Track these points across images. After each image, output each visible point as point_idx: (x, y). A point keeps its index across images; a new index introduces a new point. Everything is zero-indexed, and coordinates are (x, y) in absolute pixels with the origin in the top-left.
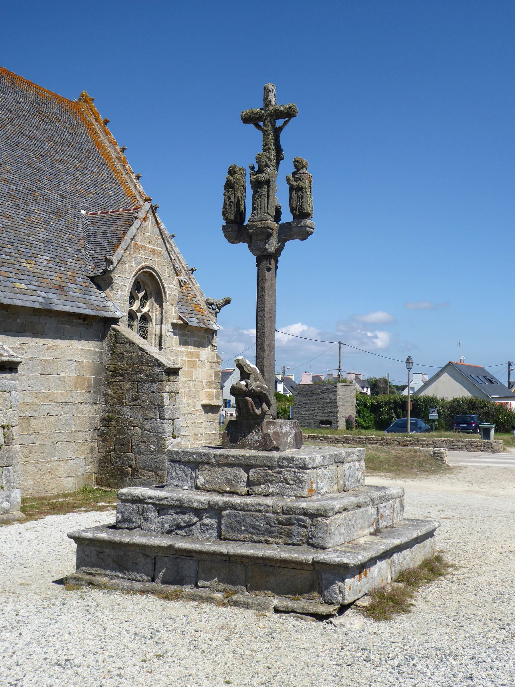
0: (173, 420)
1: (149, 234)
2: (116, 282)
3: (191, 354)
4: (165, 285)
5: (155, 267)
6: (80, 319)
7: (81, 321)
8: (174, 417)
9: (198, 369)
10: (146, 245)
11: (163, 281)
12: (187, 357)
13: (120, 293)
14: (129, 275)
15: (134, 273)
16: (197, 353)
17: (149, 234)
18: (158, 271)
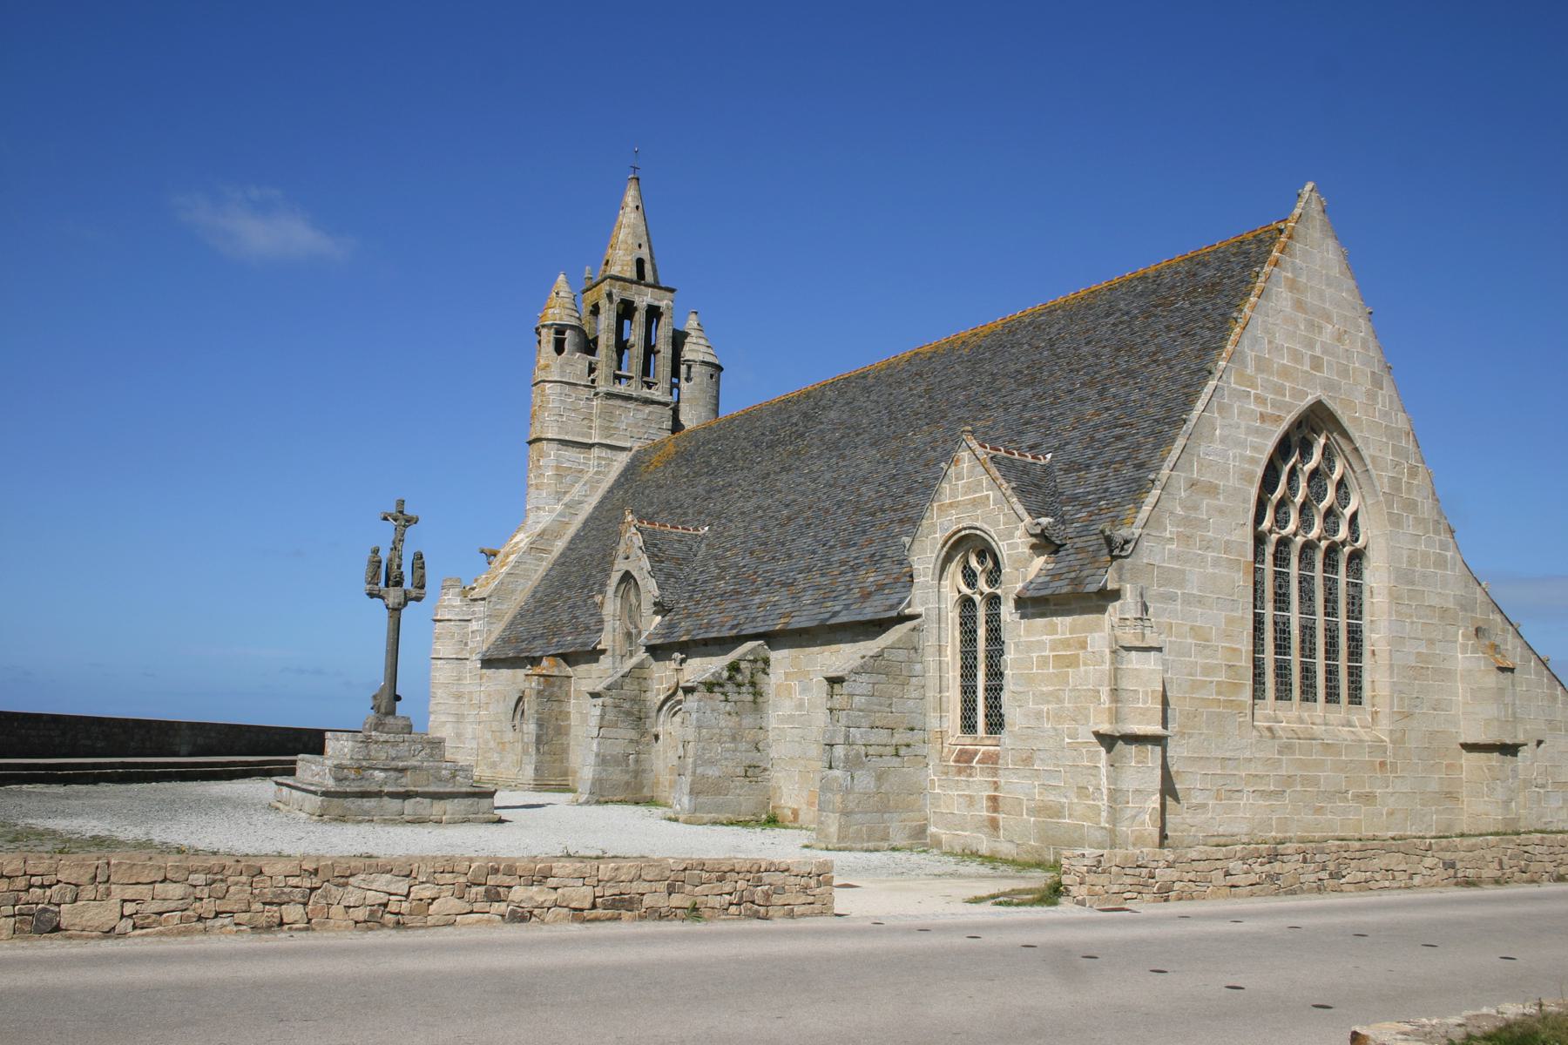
0: (833, 745)
1: (965, 481)
2: (916, 567)
3: (1066, 644)
4: (1000, 544)
5: (978, 524)
6: (875, 626)
7: (877, 629)
8: (833, 743)
9: (1082, 668)
10: (960, 499)
11: (996, 538)
12: (1053, 650)
13: (922, 579)
14: (932, 552)
15: (939, 546)
16: (1081, 639)
17: (965, 481)
18: (985, 527)
